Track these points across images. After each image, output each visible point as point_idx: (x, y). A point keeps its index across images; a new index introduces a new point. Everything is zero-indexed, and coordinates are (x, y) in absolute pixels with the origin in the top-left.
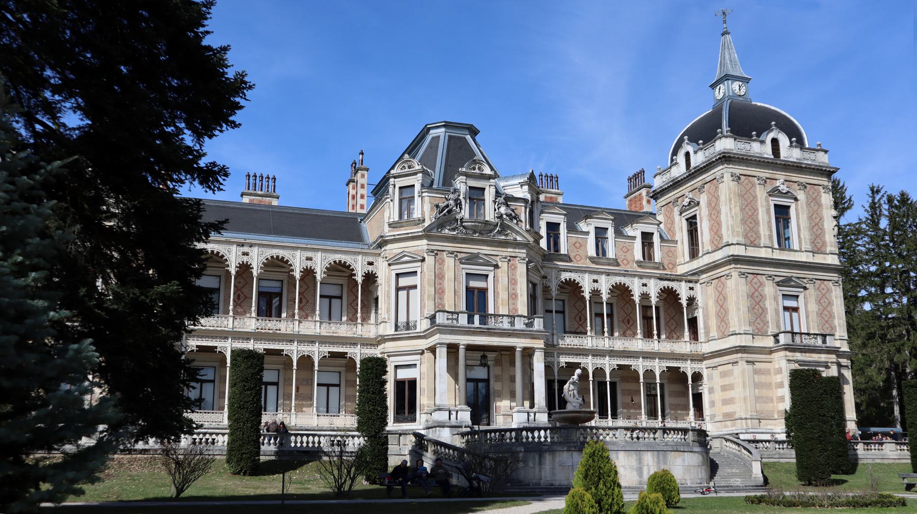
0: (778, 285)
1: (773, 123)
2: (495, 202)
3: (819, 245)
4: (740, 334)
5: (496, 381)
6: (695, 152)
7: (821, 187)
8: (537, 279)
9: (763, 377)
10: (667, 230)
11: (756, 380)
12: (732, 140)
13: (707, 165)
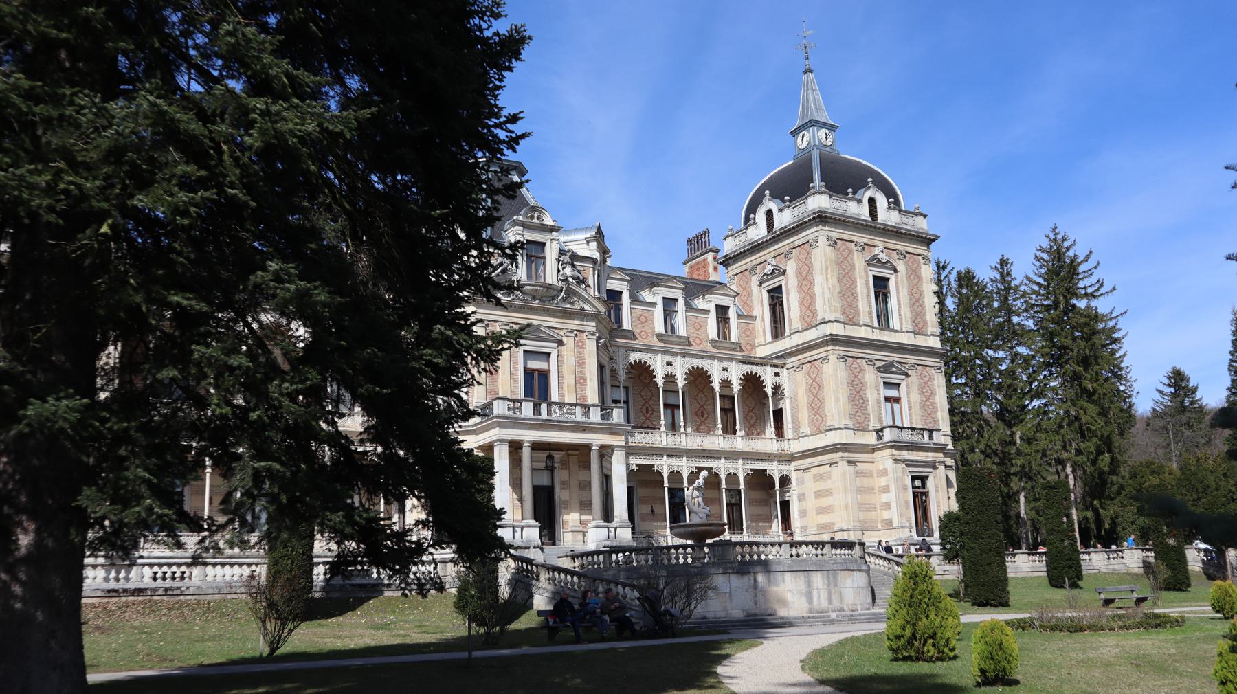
0: (879, 371)
1: (870, 180)
2: (558, 261)
3: (920, 325)
4: (840, 429)
5: (562, 489)
6: (781, 210)
7: (920, 257)
8: (605, 361)
9: (865, 480)
10: (742, 303)
11: (858, 484)
12: (828, 197)
13: (797, 226)
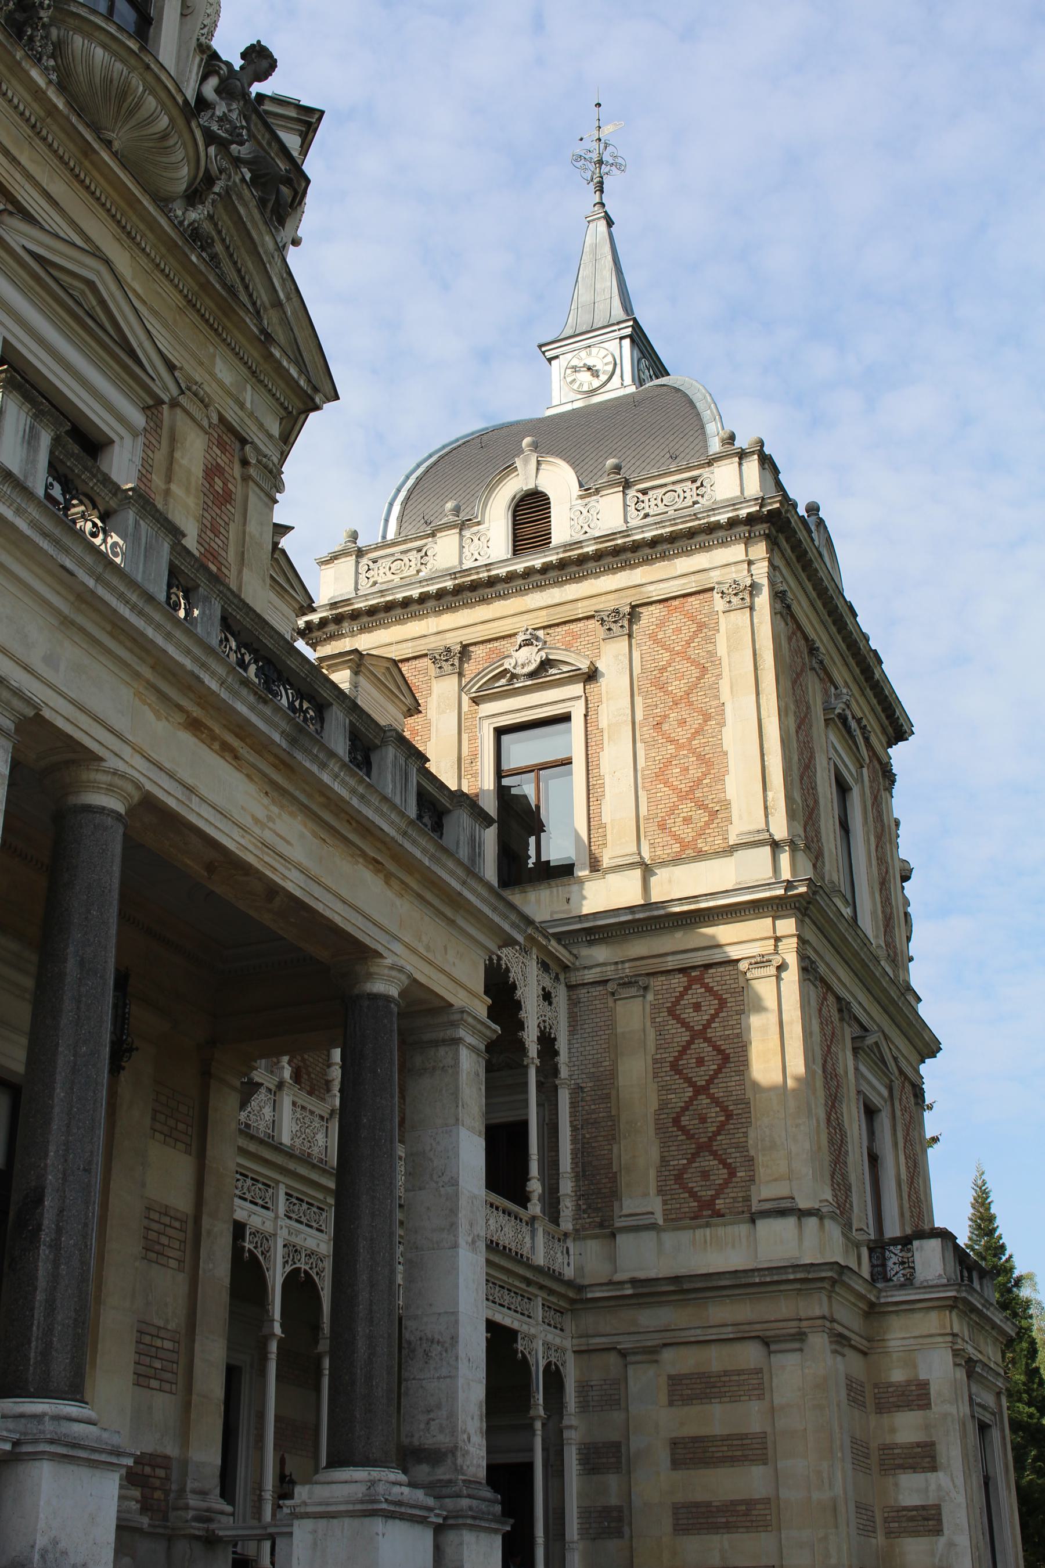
6: (588, 491)
